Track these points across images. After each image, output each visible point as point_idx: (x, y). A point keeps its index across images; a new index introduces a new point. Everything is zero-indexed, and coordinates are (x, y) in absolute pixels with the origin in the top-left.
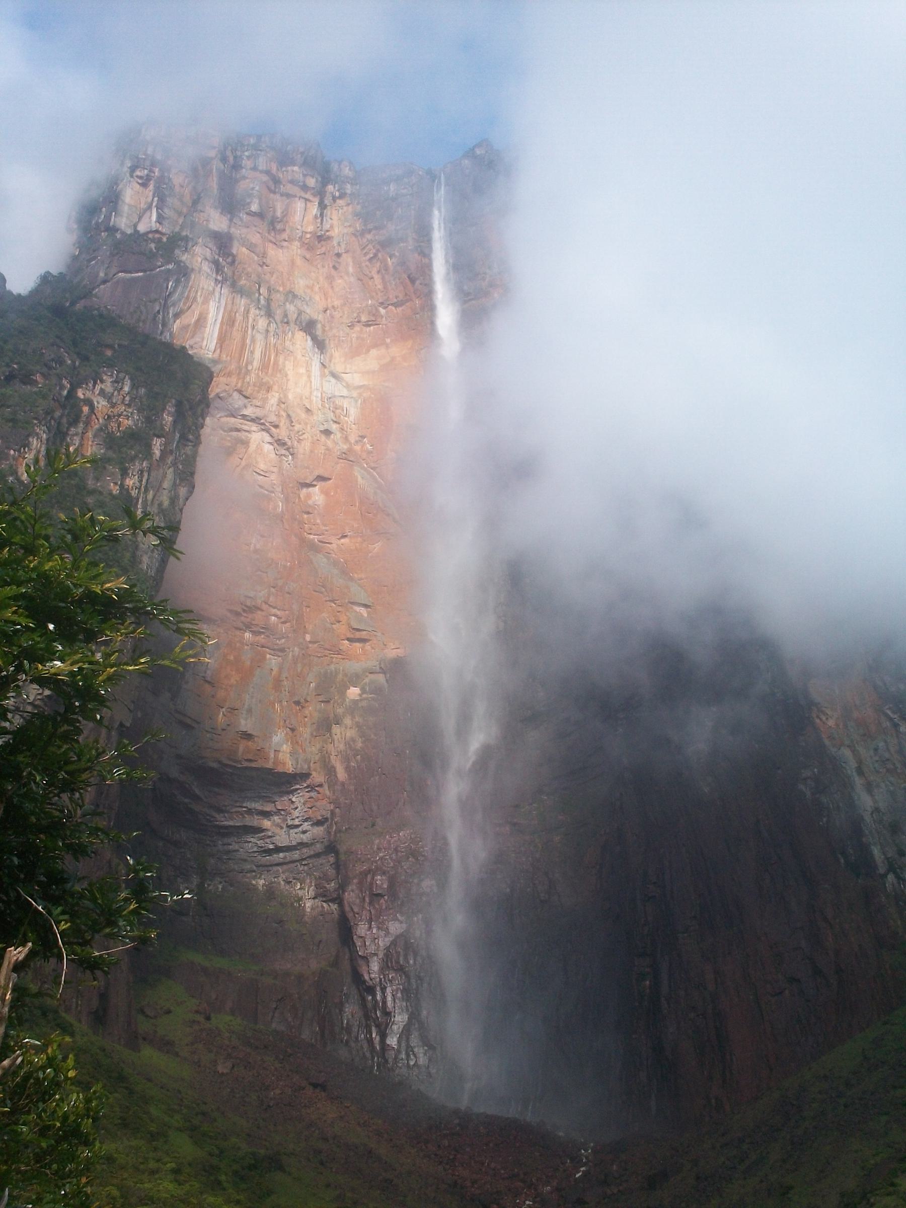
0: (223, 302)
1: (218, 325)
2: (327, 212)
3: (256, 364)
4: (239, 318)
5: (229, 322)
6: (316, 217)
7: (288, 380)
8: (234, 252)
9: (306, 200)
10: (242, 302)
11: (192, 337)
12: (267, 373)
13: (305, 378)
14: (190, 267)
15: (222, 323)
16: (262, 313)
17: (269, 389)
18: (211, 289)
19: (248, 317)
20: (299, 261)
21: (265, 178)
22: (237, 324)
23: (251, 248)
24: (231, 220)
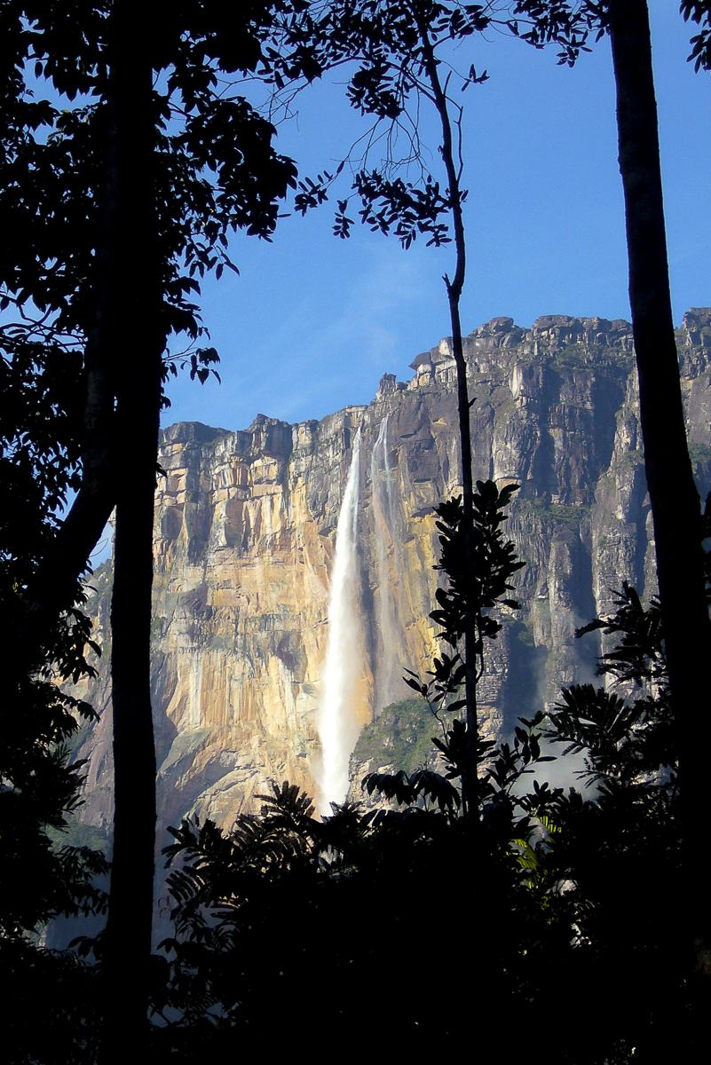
0: (201, 668)
1: (199, 695)
2: (291, 498)
3: (236, 716)
4: (217, 674)
5: (208, 684)
6: (282, 511)
7: (266, 716)
8: (209, 604)
9: (272, 495)
10: (217, 656)
11: (181, 718)
12: (246, 720)
13: (280, 707)
14: (166, 652)
15: (203, 691)
16: (239, 655)
17: (249, 736)
18: (188, 662)
19: (225, 669)
20: (273, 572)
21: (233, 492)
22: (215, 683)
23: (226, 584)
24: (205, 567)
